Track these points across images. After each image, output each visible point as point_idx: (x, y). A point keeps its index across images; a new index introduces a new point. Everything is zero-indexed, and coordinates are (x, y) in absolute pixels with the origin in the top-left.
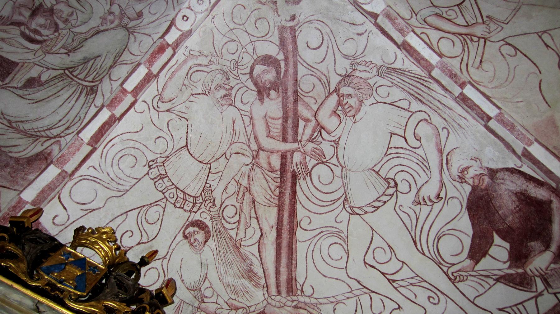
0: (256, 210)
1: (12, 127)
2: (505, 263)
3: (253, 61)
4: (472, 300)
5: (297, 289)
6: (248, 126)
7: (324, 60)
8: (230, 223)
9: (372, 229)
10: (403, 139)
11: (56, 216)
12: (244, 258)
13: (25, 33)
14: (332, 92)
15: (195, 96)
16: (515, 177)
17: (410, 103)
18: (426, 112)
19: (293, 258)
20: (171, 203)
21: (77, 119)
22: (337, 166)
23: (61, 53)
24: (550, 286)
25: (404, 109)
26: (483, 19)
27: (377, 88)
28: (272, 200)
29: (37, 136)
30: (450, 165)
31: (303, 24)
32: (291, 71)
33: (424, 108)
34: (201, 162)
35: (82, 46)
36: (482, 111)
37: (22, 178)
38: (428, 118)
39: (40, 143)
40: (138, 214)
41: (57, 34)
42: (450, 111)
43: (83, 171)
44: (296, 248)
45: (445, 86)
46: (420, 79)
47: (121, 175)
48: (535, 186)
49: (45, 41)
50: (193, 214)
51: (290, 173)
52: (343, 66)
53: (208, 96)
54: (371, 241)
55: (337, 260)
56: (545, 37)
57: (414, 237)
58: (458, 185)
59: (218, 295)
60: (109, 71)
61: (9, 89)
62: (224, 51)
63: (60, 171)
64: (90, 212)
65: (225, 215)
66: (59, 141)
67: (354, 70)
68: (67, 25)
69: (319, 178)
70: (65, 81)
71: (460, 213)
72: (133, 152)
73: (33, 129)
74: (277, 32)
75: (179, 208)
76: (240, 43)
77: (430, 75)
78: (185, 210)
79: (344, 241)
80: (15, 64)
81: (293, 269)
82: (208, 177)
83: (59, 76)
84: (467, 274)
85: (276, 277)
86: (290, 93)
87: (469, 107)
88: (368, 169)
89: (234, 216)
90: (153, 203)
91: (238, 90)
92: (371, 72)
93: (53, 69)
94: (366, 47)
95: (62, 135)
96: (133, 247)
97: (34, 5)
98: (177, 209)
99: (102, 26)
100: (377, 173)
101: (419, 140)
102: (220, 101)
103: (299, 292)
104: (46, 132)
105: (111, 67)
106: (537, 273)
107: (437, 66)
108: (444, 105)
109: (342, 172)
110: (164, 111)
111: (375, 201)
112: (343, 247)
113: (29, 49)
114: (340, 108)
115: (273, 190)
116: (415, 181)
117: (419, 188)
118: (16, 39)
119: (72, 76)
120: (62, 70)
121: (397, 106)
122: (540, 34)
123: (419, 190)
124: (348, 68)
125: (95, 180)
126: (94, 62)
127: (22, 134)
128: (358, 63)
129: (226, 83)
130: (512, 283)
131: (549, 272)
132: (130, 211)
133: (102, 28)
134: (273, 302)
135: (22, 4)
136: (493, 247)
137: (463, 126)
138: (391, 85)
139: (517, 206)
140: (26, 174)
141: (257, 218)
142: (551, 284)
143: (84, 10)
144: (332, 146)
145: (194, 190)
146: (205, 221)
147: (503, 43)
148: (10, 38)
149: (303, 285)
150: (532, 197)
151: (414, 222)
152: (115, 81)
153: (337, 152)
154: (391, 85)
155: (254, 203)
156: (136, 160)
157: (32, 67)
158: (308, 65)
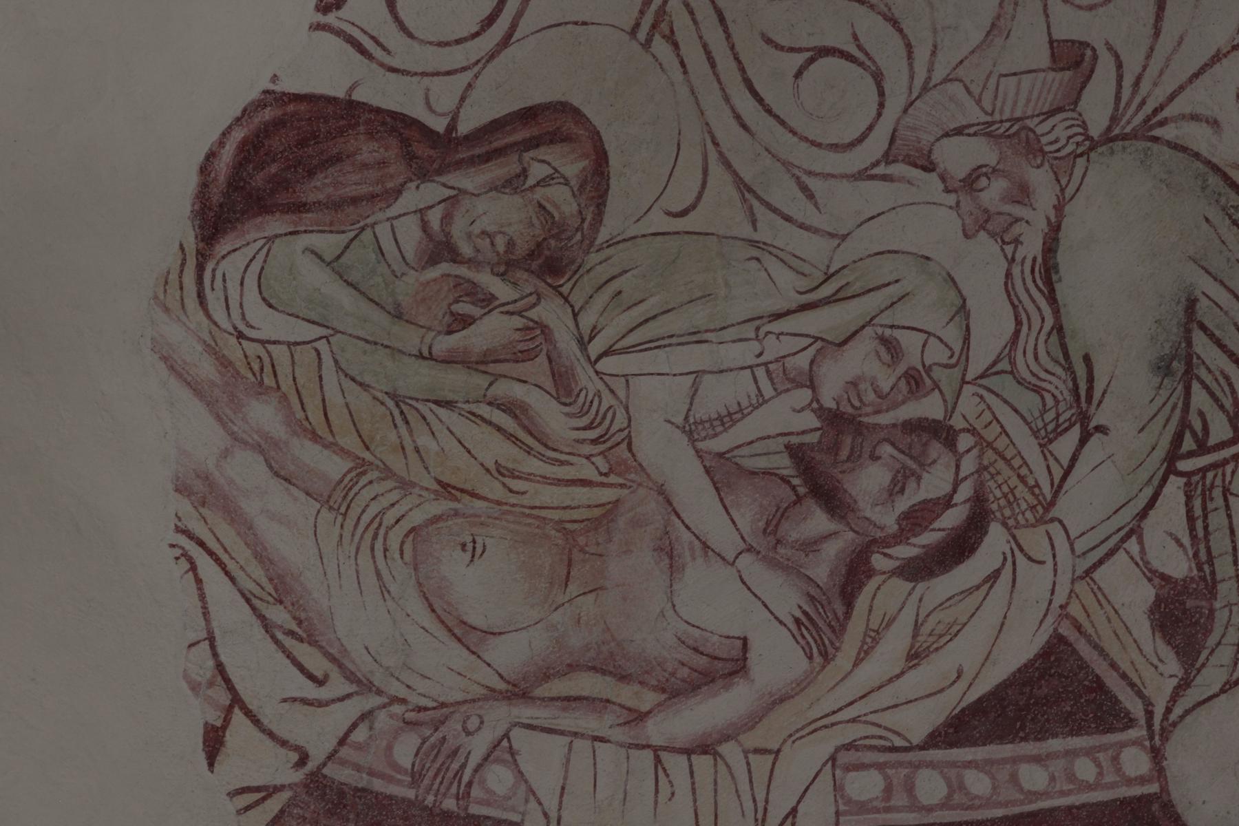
23: (1074, 459)
35: (1087, 359)
41: (965, 441)
61: (1178, 711)
68: (936, 386)
83: (1197, 503)
93: (1143, 514)
97: (784, 480)
99: (1017, 241)
113: (995, 575)
118: (928, 605)
120: (1164, 480)
126: (1211, 336)
133: (1032, 246)
135: (762, 524)
148: (917, 627)
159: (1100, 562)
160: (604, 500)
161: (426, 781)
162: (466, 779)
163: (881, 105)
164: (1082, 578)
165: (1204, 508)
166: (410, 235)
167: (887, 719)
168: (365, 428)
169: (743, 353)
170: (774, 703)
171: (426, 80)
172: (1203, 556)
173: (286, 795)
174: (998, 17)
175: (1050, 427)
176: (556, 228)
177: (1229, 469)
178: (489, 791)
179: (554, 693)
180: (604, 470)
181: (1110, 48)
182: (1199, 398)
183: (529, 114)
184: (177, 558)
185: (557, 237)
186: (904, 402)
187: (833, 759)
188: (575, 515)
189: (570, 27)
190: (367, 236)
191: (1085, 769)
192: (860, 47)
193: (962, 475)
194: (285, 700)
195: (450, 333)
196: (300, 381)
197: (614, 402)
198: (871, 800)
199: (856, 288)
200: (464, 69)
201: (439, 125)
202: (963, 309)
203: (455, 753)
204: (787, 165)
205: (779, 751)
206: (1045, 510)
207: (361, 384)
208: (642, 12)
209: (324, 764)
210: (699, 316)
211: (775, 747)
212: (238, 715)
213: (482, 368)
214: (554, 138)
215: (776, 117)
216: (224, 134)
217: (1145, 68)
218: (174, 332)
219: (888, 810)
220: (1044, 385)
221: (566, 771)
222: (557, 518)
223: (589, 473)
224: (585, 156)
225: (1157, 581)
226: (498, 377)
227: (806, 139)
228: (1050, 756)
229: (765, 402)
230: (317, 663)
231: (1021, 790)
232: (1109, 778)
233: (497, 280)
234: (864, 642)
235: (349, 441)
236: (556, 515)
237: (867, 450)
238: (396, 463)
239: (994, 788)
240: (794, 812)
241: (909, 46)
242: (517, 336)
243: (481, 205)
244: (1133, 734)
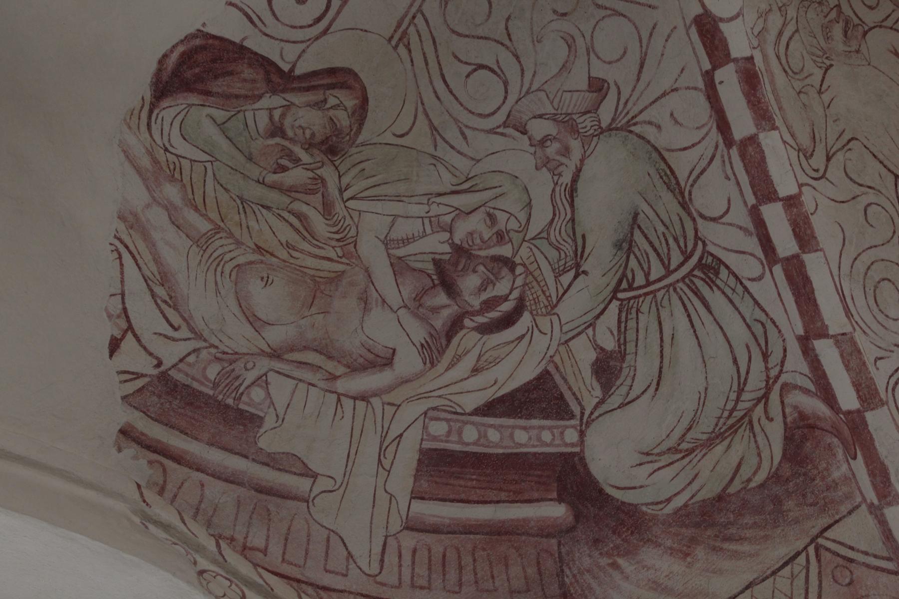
1: (690, 452)
15: (823, 89)
21: (758, 329)
23: (570, 286)
29: (742, 418)
35: (584, 237)
37: (828, 488)
39: (764, 421)
41: (519, 270)
49: (521, 300)
53: (831, 65)
60: (690, 214)
61: (596, 414)
68: (511, 240)
70: (645, 308)
73: (720, 418)
80: (544, 378)
83: (624, 315)
95: (773, 373)
97: (429, 276)
99: (560, 175)
102: (848, 49)
105: (684, 206)
110: (827, 167)
113: (523, 336)
118: (488, 346)
120: (610, 301)
127: (718, 441)
129: (826, 10)
133: (567, 179)
135: (414, 296)
140: (823, 479)
143: (498, 191)
148: (480, 356)
156: (889, 280)
157: (569, 351)
159: (573, 338)
160: (337, 270)
161: (220, 388)
162: (241, 391)
163: (506, 98)
164: (563, 344)
165: (626, 318)
166: (263, 120)
168: (223, 211)
169: (420, 210)
170: (402, 383)
171: (283, 44)
172: (622, 341)
173: (147, 380)
174: (567, 62)
175: (561, 268)
176: (337, 132)
177: (641, 299)
178: (251, 399)
179: (294, 359)
180: (340, 254)
181: (616, 84)
182: (633, 263)
183: (332, 72)
184: (112, 251)
185: (337, 136)
186: (493, 246)
187: (425, 413)
188: (322, 274)
189: (358, 31)
190: (241, 115)
191: (546, 436)
192: (499, 67)
193: (515, 286)
194: (155, 334)
195: (275, 173)
196: (194, 180)
197: (351, 223)
198: (440, 436)
199: (480, 187)
200: (302, 42)
201: (286, 68)
202: (529, 204)
203: (238, 378)
204: (456, 121)
205: (400, 405)
206: (552, 308)
207: (225, 189)
208: (395, 31)
209: (170, 369)
210: (402, 188)
211: (399, 404)
212: (130, 335)
213: (288, 193)
214: (343, 86)
215: (454, 95)
216: (174, 47)
217: (631, 96)
218: (131, 140)
219: (447, 441)
220: (561, 247)
221: (292, 397)
222: (312, 274)
223: (332, 255)
224: (357, 98)
225: (598, 350)
226: (295, 199)
227: (467, 109)
229: (426, 236)
230: (176, 320)
231: (514, 441)
232: (557, 442)
233: (303, 152)
234: (452, 360)
235: (214, 215)
236: (312, 272)
237: (472, 267)
238: (237, 232)
239: (501, 439)
240: (401, 435)
241: (522, 70)
242: (309, 181)
243: (301, 113)
244: (573, 422)
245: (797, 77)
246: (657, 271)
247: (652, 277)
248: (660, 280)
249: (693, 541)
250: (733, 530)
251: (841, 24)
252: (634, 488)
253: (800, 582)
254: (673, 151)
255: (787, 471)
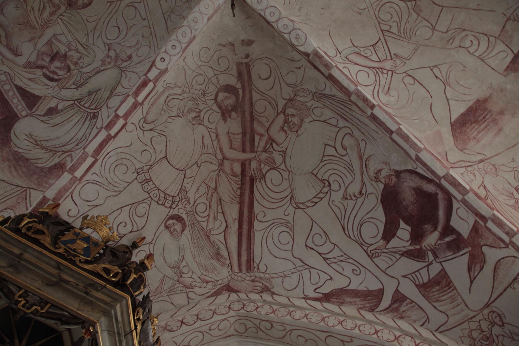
0: (222, 207)
1: (38, 145)
2: (407, 241)
3: (217, 90)
4: (384, 271)
5: (254, 267)
6: (214, 140)
7: (272, 88)
8: (201, 217)
9: (312, 219)
10: (334, 149)
11: (70, 210)
12: (213, 244)
13: (46, 74)
14: (280, 113)
15: (171, 118)
16: (413, 177)
17: (338, 121)
18: (349, 128)
19: (252, 244)
20: (155, 201)
21: (84, 138)
22: (286, 171)
24: (437, 257)
25: (334, 125)
26: (391, 56)
27: (313, 110)
28: (234, 198)
29: (56, 151)
30: (368, 168)
31: (255, 60)
32: (247, 96)
33: (347, 124)
34: (178, 169)
36: (387, 127)
38: (351, 132)
39: (58, 157)
40: (130, 210)
41: (69, 74)
42: (366, 127)
43: (88, 177)
44: (254, 236)
45: (361, 107)
46: (344, 102)
47: (116, 179)
48: (426, 183)
49: (60, 79)
50: (172, 210)
51: (248, 177)
52: (287, 92)
53: (181, 117)
54: (311, 229)
55: (285, 244)
56: (435, 70)
57: (343, 225)
58: (374, 184)
59: (193, 272)
60: (106, 101)
61: (35, 116)
62: (194, 82)
63: (72, 176)
64: (94, 207)
65: (197, 211)
66: (71, 154)
67: (296, 95)
68: (76, 67)
69: (271, 181)
70: (75, 109)
71: (376, 205)
72: (125, 162)
74: (235, 68)
75: (161, 205)
76: (206, 76)
77: (350, 99)
78: (166, 207)
79: (291, 229)
80: (38, 98)
81: (252, 252)
82: (183, 181)
84: (381, 252)
85: (238, 258)
86: (247, 114)
87: (379, 124)
88: (309, 173)
89: (205, 211)
90: (141, 201)
91: (206, 113)
92: (308, 97)
93: (66, 100)
94: (303, 78)
95: (73, 150)
96: (126, 234)
97: (52, 52)
98: (160, 206)
99: (102, 66)
100: (316, 176)
101: (345, 149)
103: (256, 270)
104: (62, 148)
105: (108, 98)
106: (429, 248)
107: (354, 93)
108: (362, 122)
109: (289, 175)
110: (148, 130)
111: (314, 198)
112: (290, 234)
113: (48, 85)
114: (286, 125)
115: (235, 191)
116: (343, 181)
117: (346, 186)
119: (80, 106)
121: (329, 123)
122: (432, 68)
123: (346, 188)
124: (291, 93)
125: (96, 183)
128: (298, 90)
129: (196, 107)
130: (412, 256)
131: (437, 246)
132: (124, 207)
133: (102, 68)
134: (236, 277)
136: (399, 230)
137: (376, 138)
138: (323, 107)
139: (415, 199)
140: (48, 179)
141: (223, 213)
142: (438, 255)
144: (281, 155)
145: (173, 191)
146: (182, 215)
147: (405, 74)
149: (259, 264)
150: (425, 191)
151: (343, 213)
152: (111, 108)
153: (285, 160)
154: (323, 107)
155: (221, 201)
156: (128, 168)
158: (261, 91)
159: (56, 98)
167: (16, 78)
182: (87, 98)
187: (6, 72)
204: (101, 32)
223: (40, 22)
226: (48, 3)
228: (20, 102)
232: (20, 111)
236: (30, 20)
245: (168, 107)
246: (87, 105)
247: (85, 106)
248: (85, 107)
249: (9, 160)
250: (18, 168)
251: (197, 115)
252: (17, 137)
253: (12, 192)
254: (121, 85)
255: (45, 170)
